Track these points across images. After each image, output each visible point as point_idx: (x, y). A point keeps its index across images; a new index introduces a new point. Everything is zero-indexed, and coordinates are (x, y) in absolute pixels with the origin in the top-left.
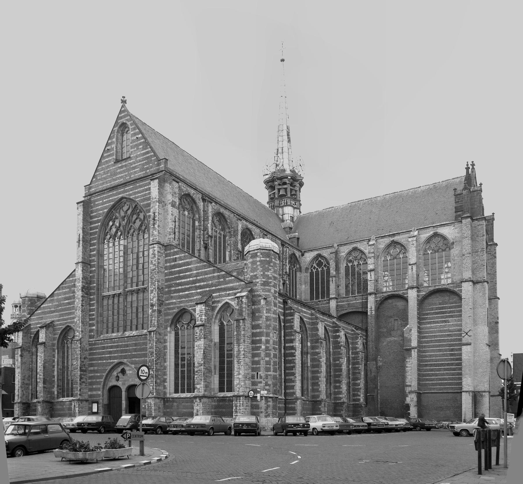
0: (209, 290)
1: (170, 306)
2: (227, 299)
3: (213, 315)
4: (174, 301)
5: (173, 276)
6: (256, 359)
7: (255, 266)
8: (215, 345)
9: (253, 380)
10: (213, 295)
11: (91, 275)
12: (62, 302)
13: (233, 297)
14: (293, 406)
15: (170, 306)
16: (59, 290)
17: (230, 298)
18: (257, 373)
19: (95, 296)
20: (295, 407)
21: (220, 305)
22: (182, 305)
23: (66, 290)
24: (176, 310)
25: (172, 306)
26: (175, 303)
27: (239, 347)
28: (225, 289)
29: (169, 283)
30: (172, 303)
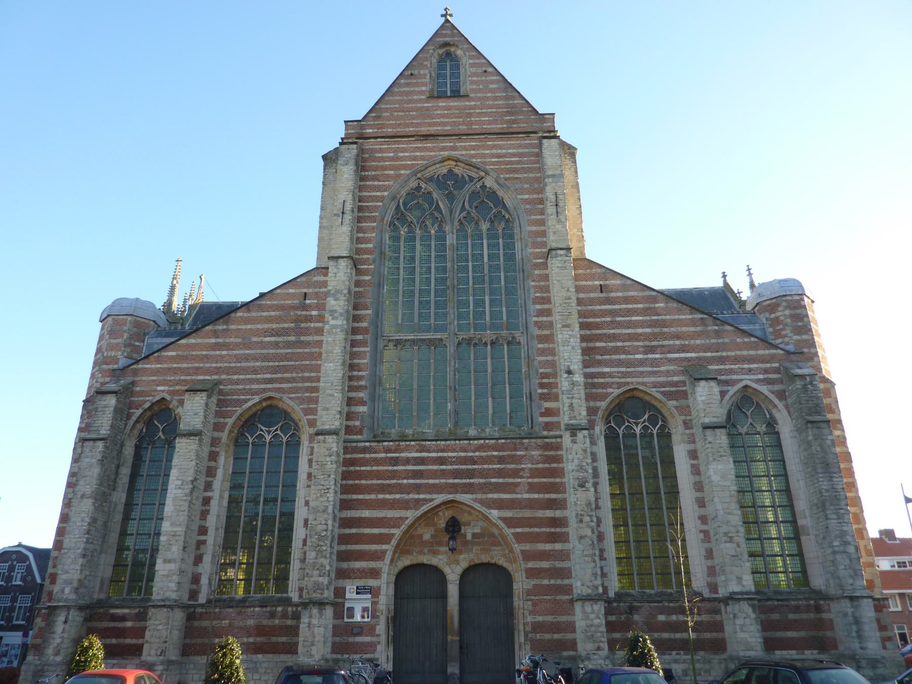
1: (596, 380)
2: (747, 380)
7: (800, 324)
12: (255, 339)
13: (761, 377)
15: (596, 380)
16: (249, 311)
19: (368, 337)
22: (629, 380)
23: (273, 313)
24: (617, 392)
25: (601, 380)
26: (610, 375)
28: (736, 360)
29: (588, 332)
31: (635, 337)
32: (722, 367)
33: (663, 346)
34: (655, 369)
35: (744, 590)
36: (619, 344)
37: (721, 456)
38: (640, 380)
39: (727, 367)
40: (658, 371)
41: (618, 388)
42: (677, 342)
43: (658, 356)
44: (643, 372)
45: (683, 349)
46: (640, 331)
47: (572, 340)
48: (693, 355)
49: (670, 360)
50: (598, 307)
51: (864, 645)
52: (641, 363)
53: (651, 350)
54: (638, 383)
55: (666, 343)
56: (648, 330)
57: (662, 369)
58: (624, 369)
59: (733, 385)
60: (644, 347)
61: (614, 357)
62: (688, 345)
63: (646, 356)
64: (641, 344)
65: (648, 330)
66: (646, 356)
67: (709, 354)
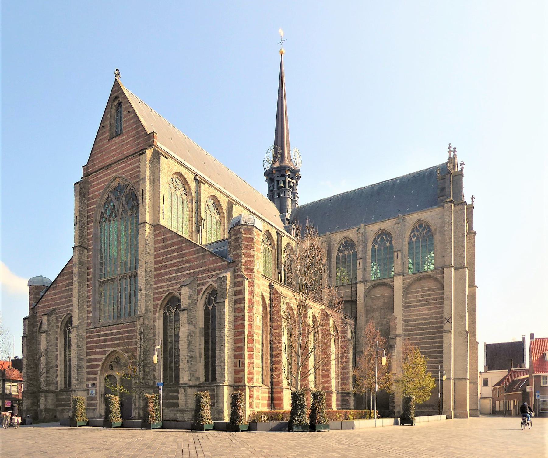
0: (194, 272)
2: (210, 281)
3: (198, 298)
4: (162, 284)
5: (161, 258)
6: (239, 345)
8: (200, 330)
9: (236, 368)
10: (198, 277)
11: (88, 260)
14: (279, 395)
17: (213, 279)
18: (240, 361)
20: (281, 397)
21: (205, 288)
22: (169, 288)
27: (220, 332)
29: (158, 266)
30: (161, 287)
31: (173, 265)
32: (203, 276)
33: (182, 268)
34: (179, 281)
35: (185, 383)
36: (167, 270)
37: (184, 324)
38: (172, 288)
39: (204, 275)
40: (179, 282)
41: (165, 293)
42: (188, 265)
43: (180, 274)
44: (174, 283)
45: (190, 268)
46: (175, 261)
47: (143, 273)
48: (193, 271)
49: (184, 275)
50: (162, 251)
51: (218, 405)
52: (174, 278)
53: (178, 271)
54: (172, 290)
55: (184, 266)
56: (178, 260)
57: (181, 280)
58: (167, 283)
59: (205, 285)
60: (176, 269)
61: (165, 277)
62: (191, 266)
63: (176, 275)
64: (174, 268)
65: (178, 260)
66: (176, 275)
67: (199, 269)
